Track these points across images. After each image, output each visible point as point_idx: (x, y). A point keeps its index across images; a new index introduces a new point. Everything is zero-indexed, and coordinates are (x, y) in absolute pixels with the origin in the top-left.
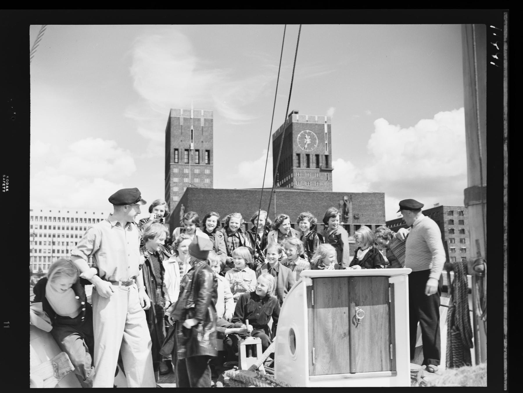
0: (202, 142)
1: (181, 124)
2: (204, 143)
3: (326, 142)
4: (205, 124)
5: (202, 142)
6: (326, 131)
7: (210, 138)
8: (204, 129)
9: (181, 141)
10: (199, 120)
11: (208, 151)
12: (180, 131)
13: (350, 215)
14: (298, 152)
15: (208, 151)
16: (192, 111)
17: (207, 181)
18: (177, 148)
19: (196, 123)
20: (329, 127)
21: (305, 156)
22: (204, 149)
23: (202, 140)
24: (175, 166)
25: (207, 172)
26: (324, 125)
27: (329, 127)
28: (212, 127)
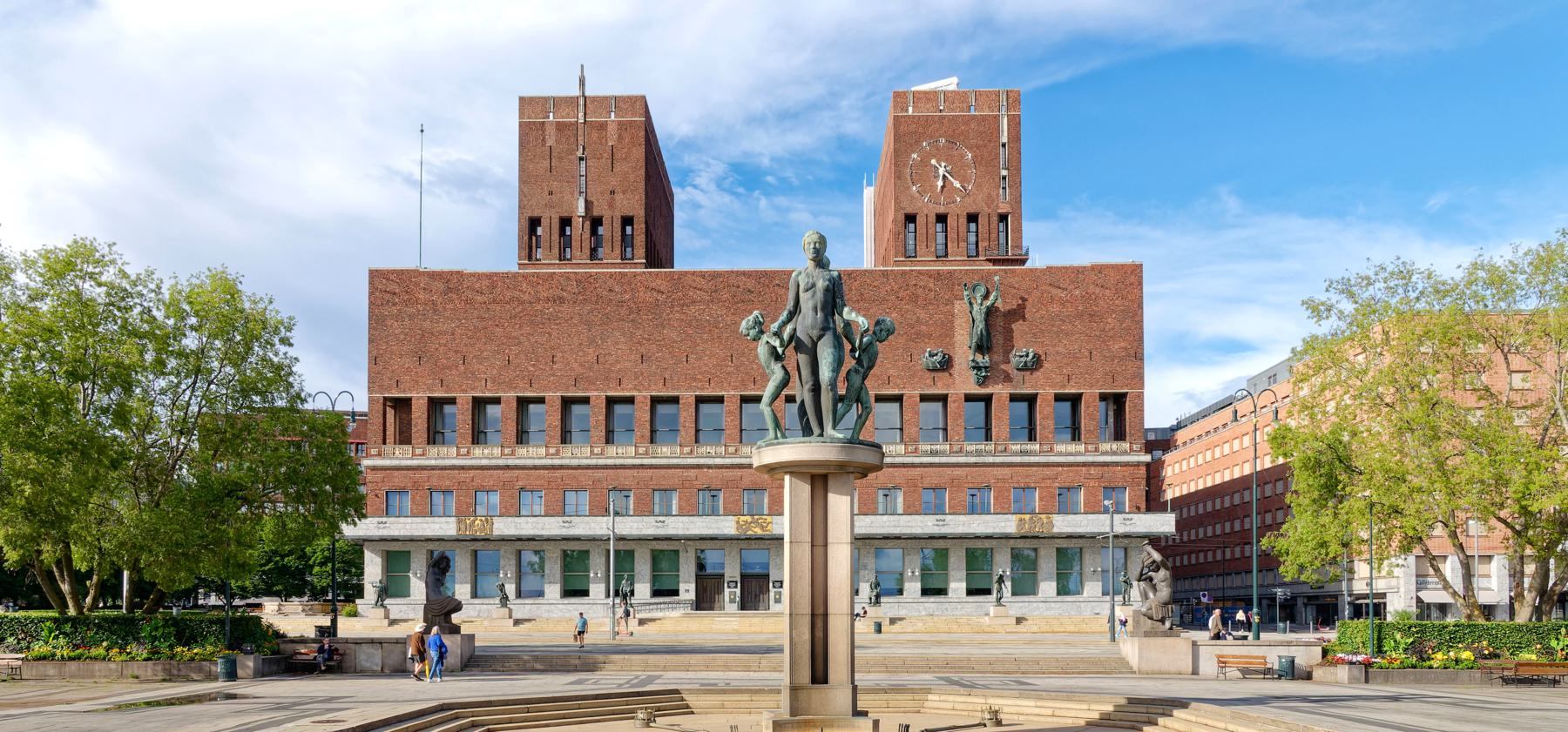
0: (612, 192)
2: (619, 197)
3: (1004, 173)
4: (620, 137)
5: (612, 192)
8: (618, 156)
9: (551, 193)
10: (602, 126)
12: (547, 163)
14: (910, 210)
18: (536, 214)
22: (618, 215)
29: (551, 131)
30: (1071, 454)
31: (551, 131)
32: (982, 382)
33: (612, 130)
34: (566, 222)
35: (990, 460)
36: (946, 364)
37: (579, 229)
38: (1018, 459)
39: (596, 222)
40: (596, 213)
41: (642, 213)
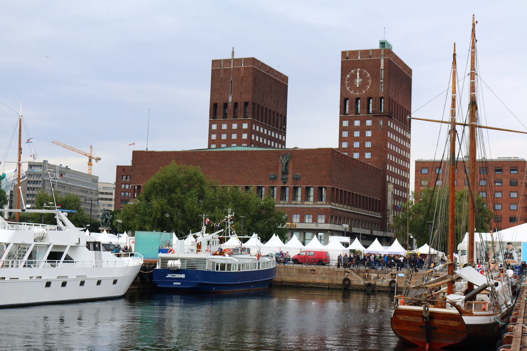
0: (241, 93)
3: (382, 81)
5: (241, 93)
9: (221, 94)
13: (290, 176)
14: (346, 97)
16: (232, 61)
21: (354, 100)
26: (380, 60)
29: (222, 72)
30: (309, 205)
31: (222, 72)
32: (285, 183)
33: (242, 70)
34: (226, 105)
35: (286, 206)
36: (275, 179)
37: (230, 106)
38: (293, 206)
39: (236, 105)
40: (235, 101)
41: (251, 101)
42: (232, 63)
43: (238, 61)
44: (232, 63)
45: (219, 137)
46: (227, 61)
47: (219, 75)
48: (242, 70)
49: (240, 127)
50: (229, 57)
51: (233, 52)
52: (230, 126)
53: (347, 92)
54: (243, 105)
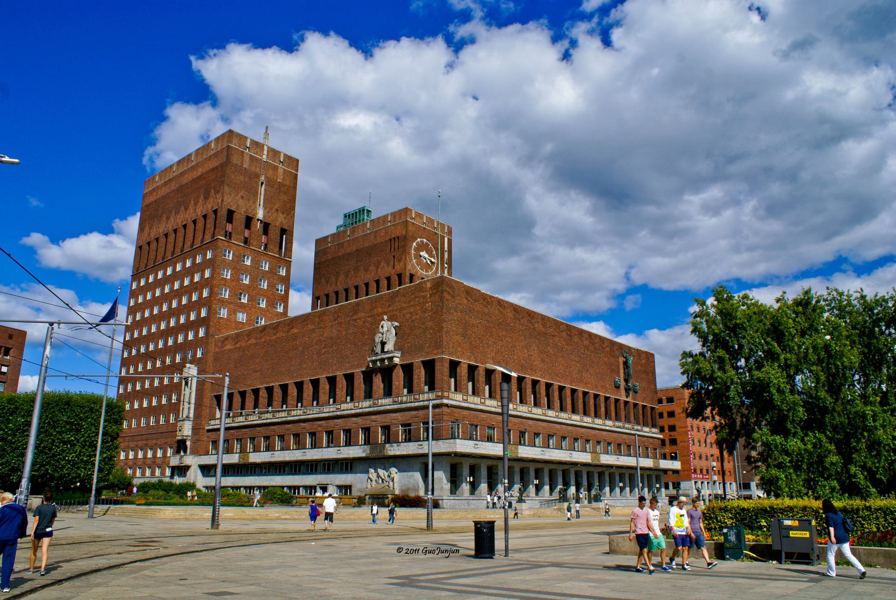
1: (244, 166)
4: (283, 179)
6: (446, 249)
7: (289, 208)
11: (283, 231)
14: (413, 272)
15: (283, 231)
16: (266, 148)
17: (281, 288)
19: (270, 172)
20: (450, 241)
23: (276, 207)
24: (226, 244)
25: (283, 273)
27: (450, 241)
28: (295, 187)
29: (247, 158)
31: (247, 158)
39: (266, 226)
42: (265, 152)
43: (274, 153)
44: (265, 152)
45: (236, 278)
46: (257, 145)
47: (242, 163)
48: (280, 171)
49: (273, 271)
50: (259, 139)
51: (266, 133)
52: (256, 263)
53: (413, 265)
54: (278, 232)
